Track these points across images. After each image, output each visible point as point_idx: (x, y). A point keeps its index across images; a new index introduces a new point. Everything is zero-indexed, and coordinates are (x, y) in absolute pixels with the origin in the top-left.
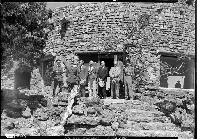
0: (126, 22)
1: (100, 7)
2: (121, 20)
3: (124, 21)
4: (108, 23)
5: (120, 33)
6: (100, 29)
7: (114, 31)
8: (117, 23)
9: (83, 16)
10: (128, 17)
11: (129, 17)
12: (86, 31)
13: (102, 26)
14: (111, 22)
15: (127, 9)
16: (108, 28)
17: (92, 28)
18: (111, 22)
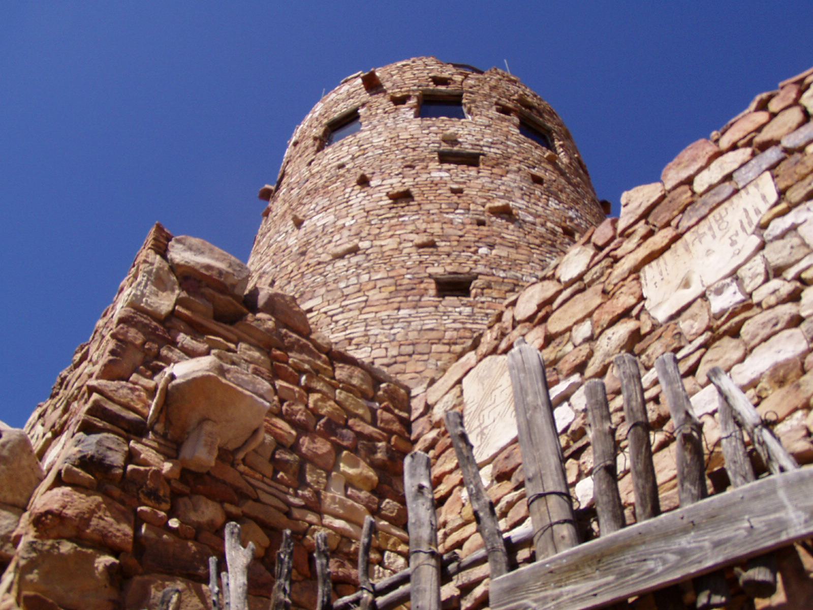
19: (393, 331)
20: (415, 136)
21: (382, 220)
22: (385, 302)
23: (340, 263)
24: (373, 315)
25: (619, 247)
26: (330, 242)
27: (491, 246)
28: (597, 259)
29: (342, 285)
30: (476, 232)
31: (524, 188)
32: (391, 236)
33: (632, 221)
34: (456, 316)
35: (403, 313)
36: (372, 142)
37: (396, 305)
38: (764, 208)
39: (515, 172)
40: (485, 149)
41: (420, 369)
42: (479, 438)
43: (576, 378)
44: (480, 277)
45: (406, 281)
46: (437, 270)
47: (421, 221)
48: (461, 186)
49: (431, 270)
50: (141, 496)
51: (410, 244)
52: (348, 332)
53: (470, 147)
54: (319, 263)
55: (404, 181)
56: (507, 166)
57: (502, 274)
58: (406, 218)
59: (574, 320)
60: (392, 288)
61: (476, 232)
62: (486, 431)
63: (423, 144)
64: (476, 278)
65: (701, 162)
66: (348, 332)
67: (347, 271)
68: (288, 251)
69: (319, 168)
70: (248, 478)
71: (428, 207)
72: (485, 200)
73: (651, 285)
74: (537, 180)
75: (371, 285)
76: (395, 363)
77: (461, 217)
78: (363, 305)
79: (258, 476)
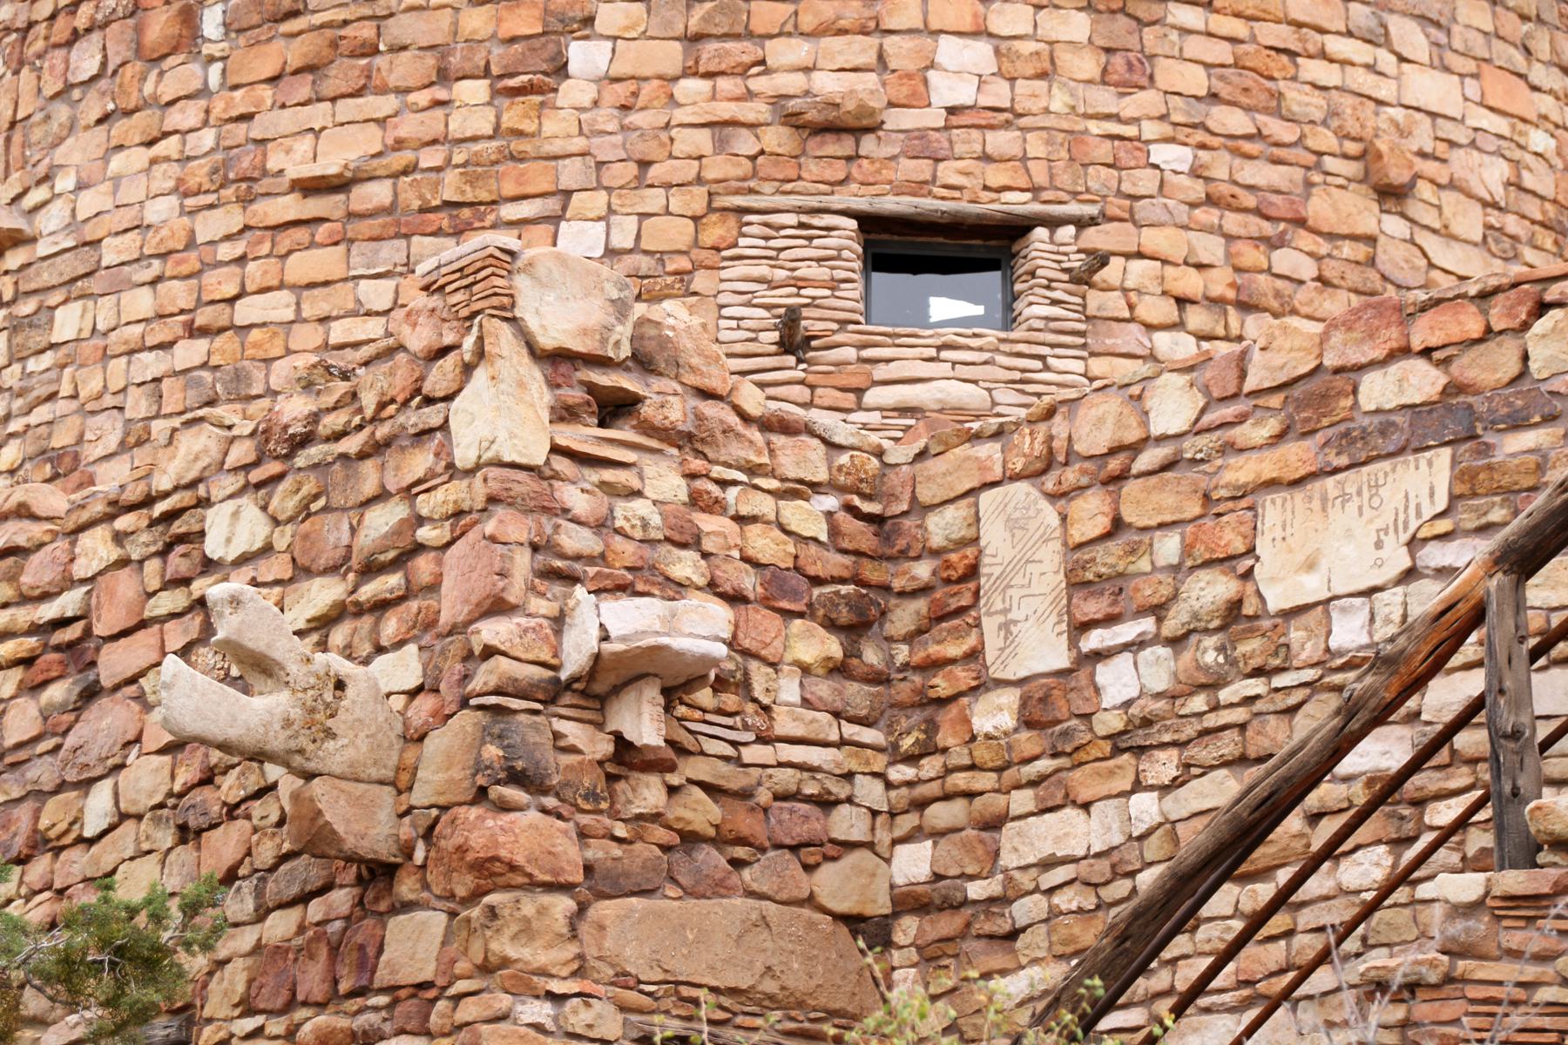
25: (1241, 423)
28: (1207, 419)
33: (1267, 385)
38: (1428, 513)
42: (1002, 633)
43: (1147, 625)
50: (579, 801)
59: (1159, 519)
62: (1012, 628)
65: (1378, 353)
70: (687, 724)
73: (1268, 537)
79: (698, 714)
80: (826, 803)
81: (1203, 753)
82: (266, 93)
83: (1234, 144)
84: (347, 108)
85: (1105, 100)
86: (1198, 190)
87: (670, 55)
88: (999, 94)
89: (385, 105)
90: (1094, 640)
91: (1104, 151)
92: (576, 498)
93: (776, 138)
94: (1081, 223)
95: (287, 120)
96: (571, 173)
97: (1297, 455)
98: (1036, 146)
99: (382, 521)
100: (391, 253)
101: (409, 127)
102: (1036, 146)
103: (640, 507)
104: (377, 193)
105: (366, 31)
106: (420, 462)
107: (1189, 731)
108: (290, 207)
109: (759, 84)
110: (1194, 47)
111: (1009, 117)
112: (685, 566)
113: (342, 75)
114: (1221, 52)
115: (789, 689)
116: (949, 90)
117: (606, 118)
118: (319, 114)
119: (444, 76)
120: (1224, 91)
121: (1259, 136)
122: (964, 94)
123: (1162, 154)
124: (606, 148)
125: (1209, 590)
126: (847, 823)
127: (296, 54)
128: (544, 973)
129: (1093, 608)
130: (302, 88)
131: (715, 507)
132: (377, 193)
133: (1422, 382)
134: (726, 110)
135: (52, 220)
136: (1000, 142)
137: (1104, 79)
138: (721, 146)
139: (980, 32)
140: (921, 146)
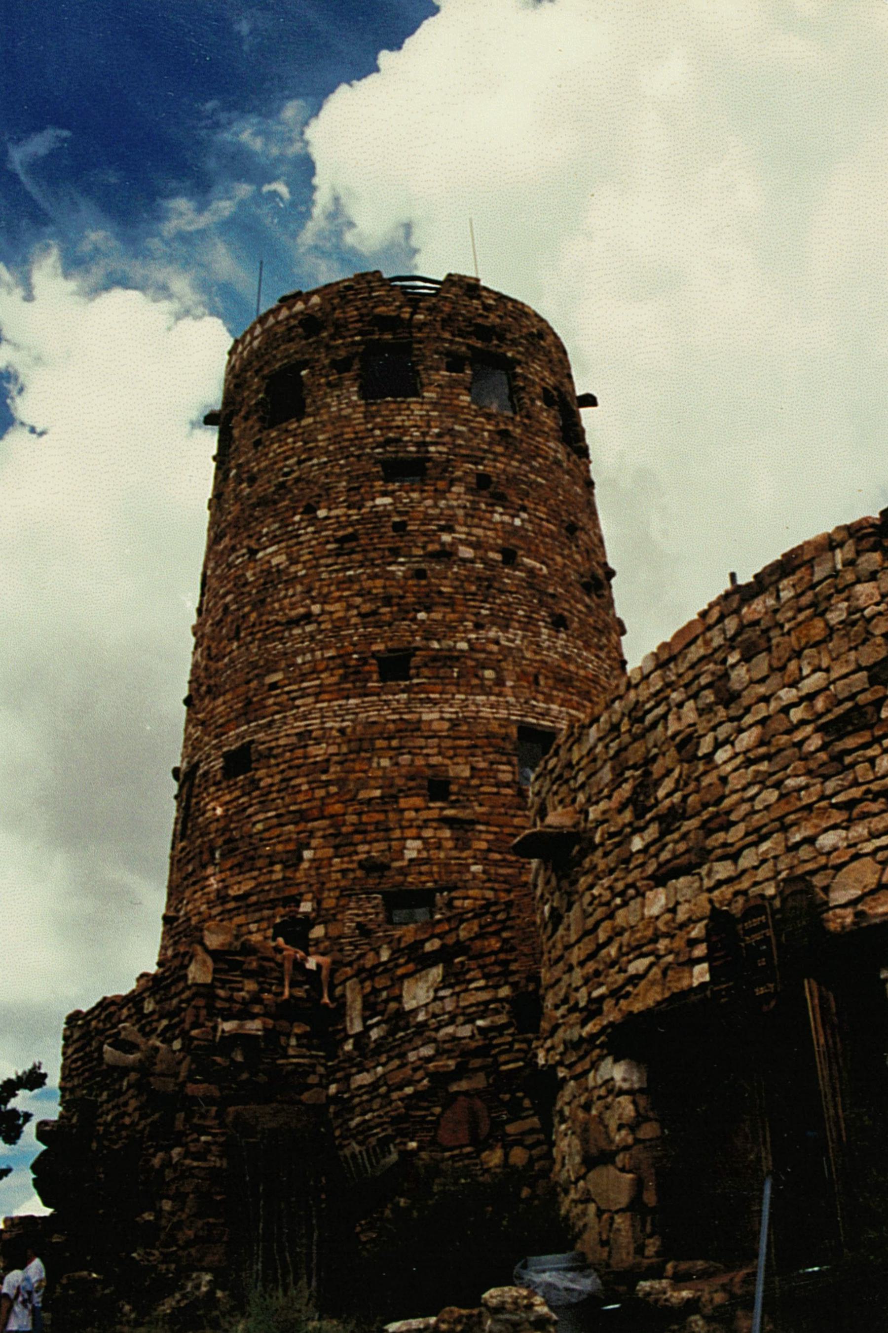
0: (849, 705)
1: (687, 678)
2: (820, 704)
3: (840, 702)
4: (748, 763)
5: (823, 804)
6: (712, 825)
7: (788, 808)
8: (798, 736)
9: (628, 774)
10: (852, 667)
11: (859, 669)
12: (651, 868)
13: (723, 797)
14: (762, 750)
15: (834, 618)
16: (752, 799)
17: (676, 836)
18: (762, 750)
19: (345, 724)
20: (360, 435)
21: (331, 572)
22: (336, 688)
23: (297, 631)
24: (325, 704)
26: (285, 597)
27: (428, 610)
29: (299, 660)
30: (415, 589)
31: (468, 504)
32: (339, 599)
34: (394, 705)
35: (352, 701)
36: (316, 441)
37: (345, 693)
39: (460, 479)
40: (432, 449)
41: (366, 767)
44: (418, 653)
45: (353, 663)
46: (378, 647)
47: (365, 576)
48: (405, 518)
49: (374, 648)
51: (355, 612)
52: (308, 722)
53: (413, 449)
54: (277, 623)
55: (351, 512)
56: (452, 472)
57: (436, 645)
58: (351, 573)
60: (341, 671)
61: (415, 589)
63: (368, 450)
64: (414, 655)
66: (308, 722)
67: (302, 642)
68: (247, 589)
69: (267, 463)
71: (373, 555)
72: (425, 539)
74: (483, 481)
75: (321, 667)
76: (346, 761)
77: (402, 568)
78: (318, 690)
80: (307, 1074)
81: (392, 1054)
82: (228, 873)
83: (496, 863)
84: (248, 875)
85: (455, 853)
86: (484, 877)
87: (330, 852)
88: (424, 854)
89: (255, 873)
90: (370, 1022)
91: (456, 868)
92: (221, 993)
93: (359, 873)
94: (450, 890)
95: (233, 880)
96: (303, 888)
97: (411, 966)
98: (435, 869)
99: (175, 1002)
100: (257, 915)
101: (262, 879)
102: (435, 869)
103: (243, 994)
104: (254, 899)
105: (252, 853)
106: (181, 985)
107: (388, 1047)
108: (232, 905)
109: (355, 858)
110: (484, 836)
111: (427, 861)
112: (257, 1009)
113: (247, 865)
114: (491, 837)
115: (293, 1042)
116: (410, 854)
117: (313, 872)
118: (240, 878)
119: (272, 864)
120: (494, 848)
121: (504, 860)
122: (414, 855)
123: (474, 868)
124: (312, 881)
125: (393, 1005)
126: (313, 1079)
127: (235, 861)
128: (211, 1127)
129: (368, 1013)
130: (237, 871)
131: (269, 991)
132: (254, 899)
133: (436, 944)
134: (345, 866)
135: (182, 913)
136: (424, 868)
137: (456, 848)
138: (344, 877)
139: (418, 837)
140: (402, 871)
